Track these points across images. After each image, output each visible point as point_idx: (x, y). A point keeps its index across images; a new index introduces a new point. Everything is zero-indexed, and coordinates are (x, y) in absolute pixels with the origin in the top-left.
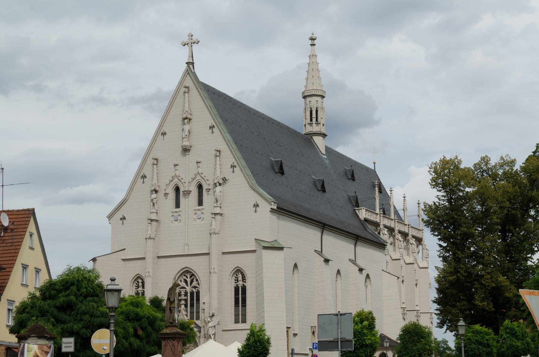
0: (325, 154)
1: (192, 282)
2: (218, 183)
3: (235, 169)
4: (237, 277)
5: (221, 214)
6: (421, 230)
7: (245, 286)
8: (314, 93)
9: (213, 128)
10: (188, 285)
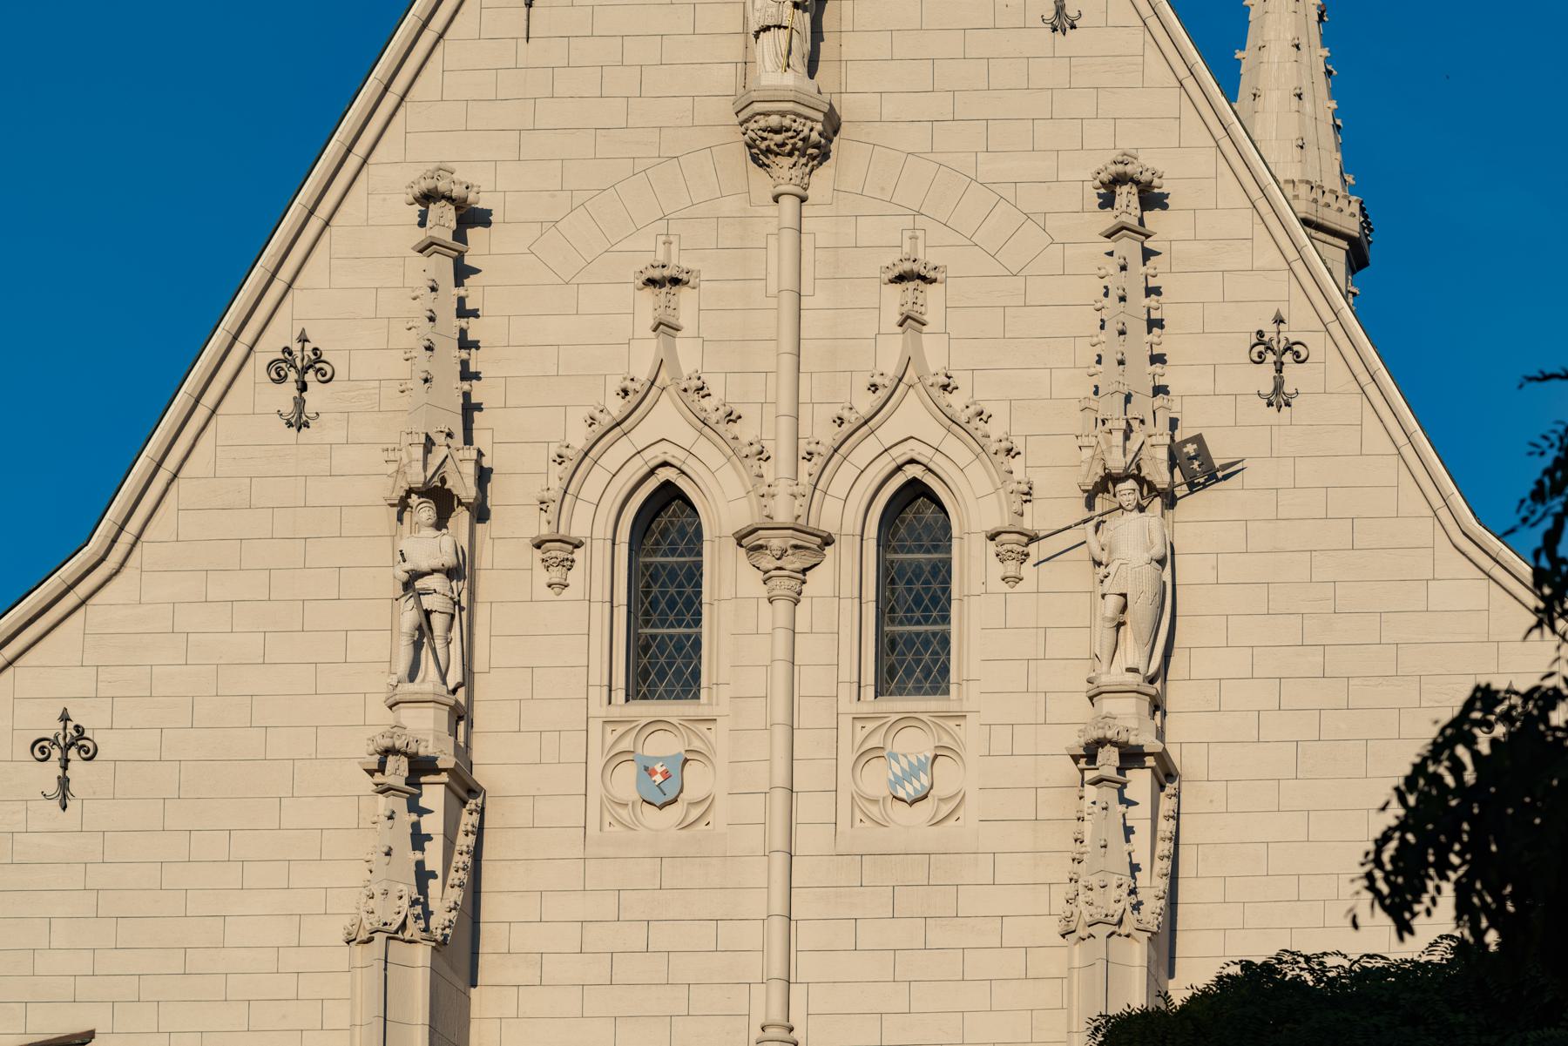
3: (1291, 370)
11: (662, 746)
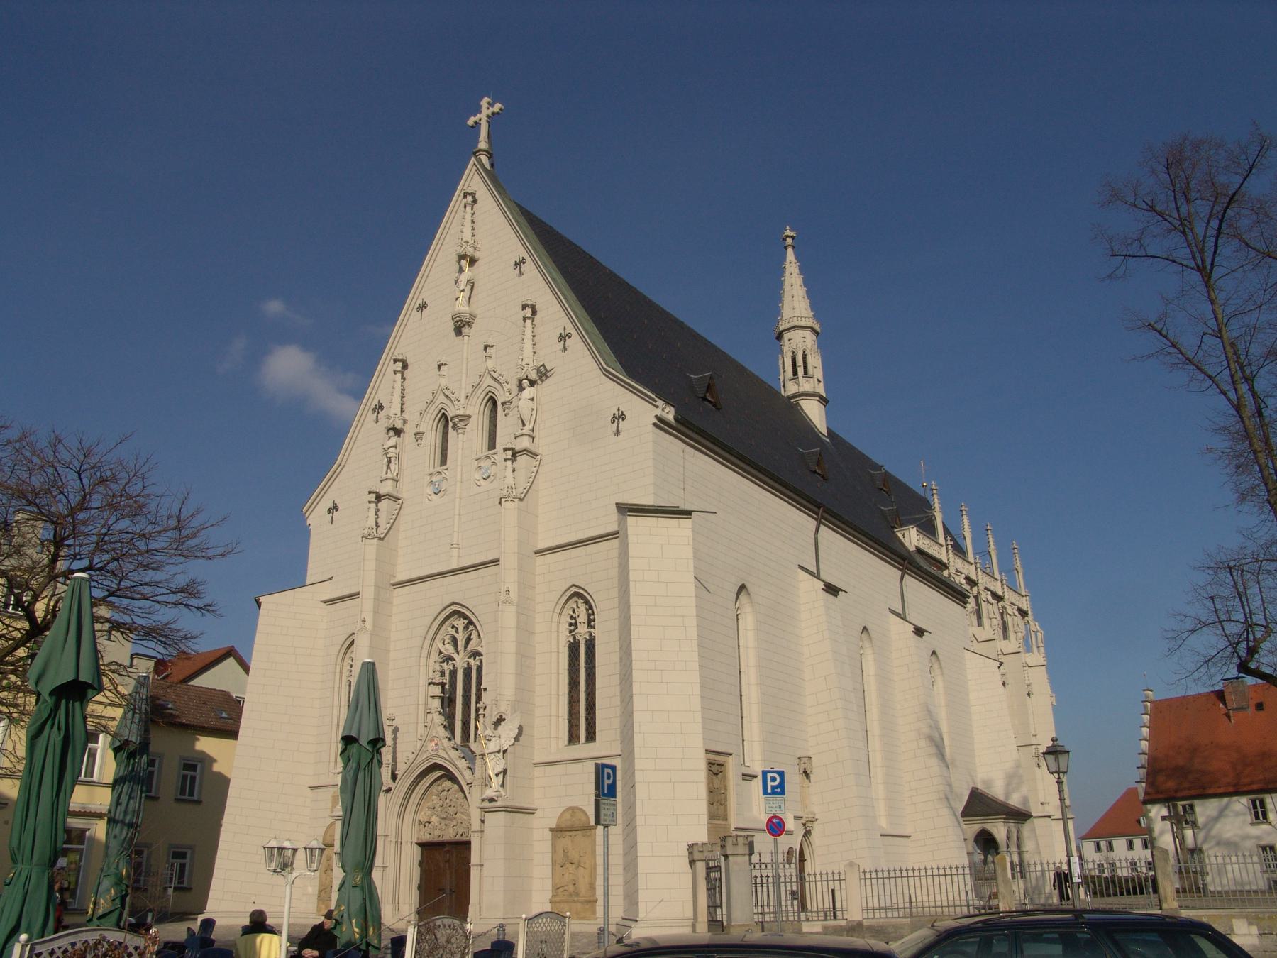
0: (826, 435)
1: (468, 640)
2: (527, 379)
3: (568, 341)
4: (574, 615)
5: (534, 455)
6: (1023, 596)
7: (594, 639)
8: (797, 323)
9: (522, 264)
10: (459, 648)
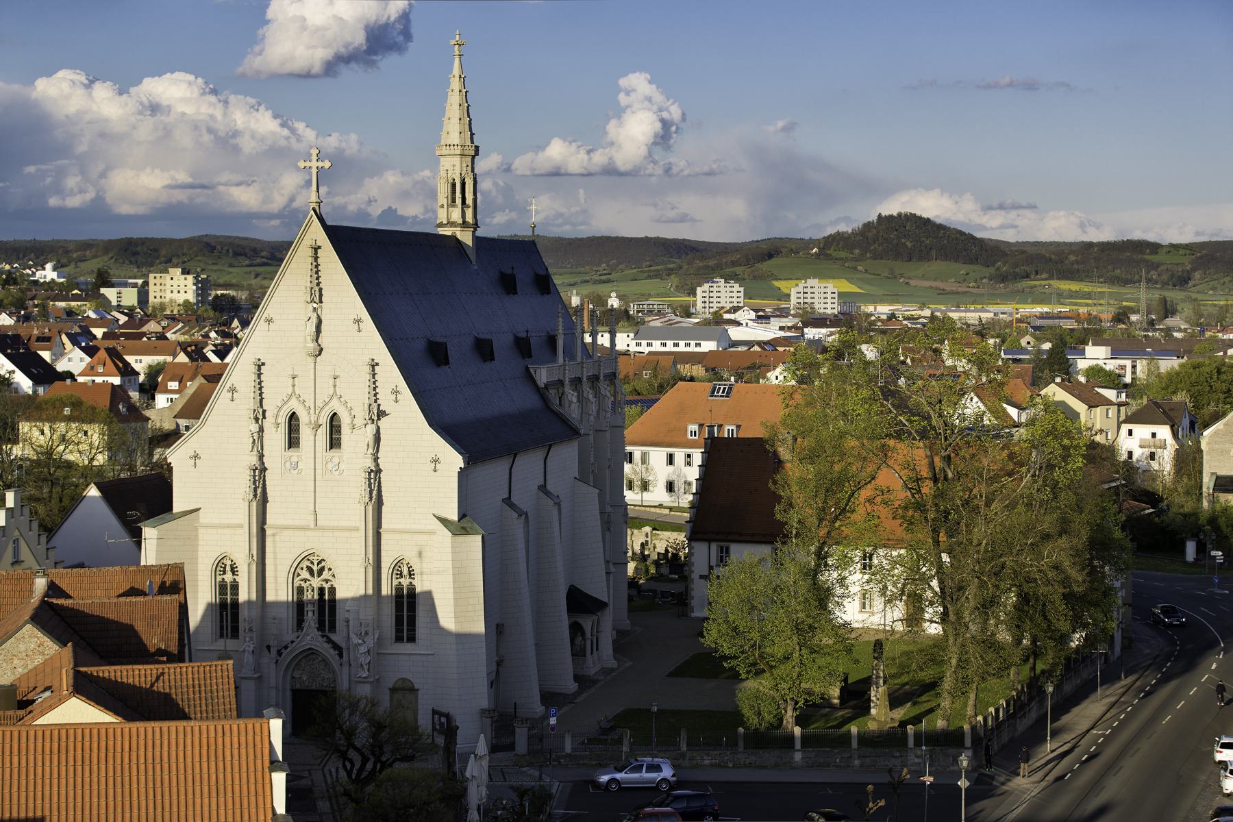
11: (294, 459)
